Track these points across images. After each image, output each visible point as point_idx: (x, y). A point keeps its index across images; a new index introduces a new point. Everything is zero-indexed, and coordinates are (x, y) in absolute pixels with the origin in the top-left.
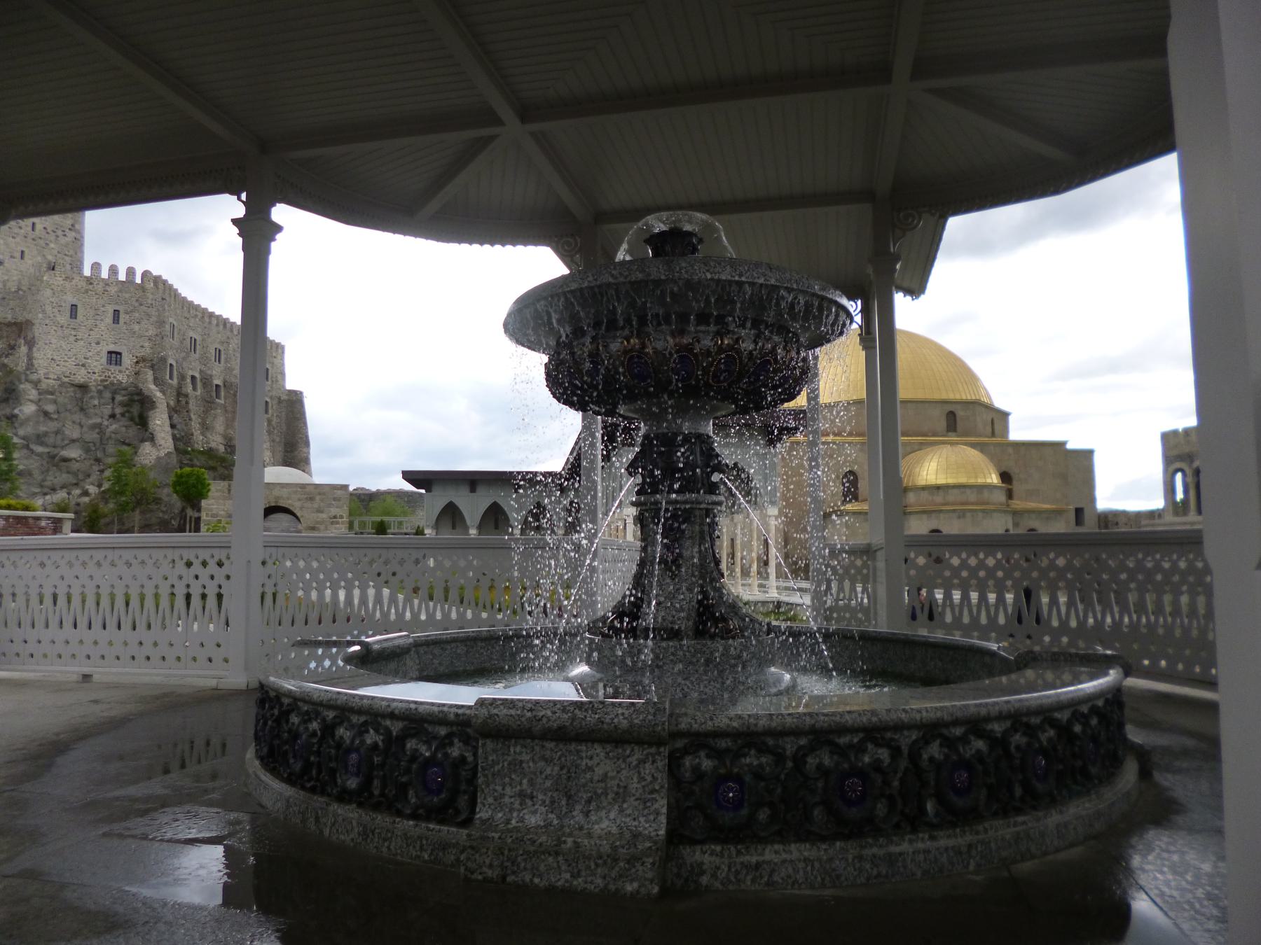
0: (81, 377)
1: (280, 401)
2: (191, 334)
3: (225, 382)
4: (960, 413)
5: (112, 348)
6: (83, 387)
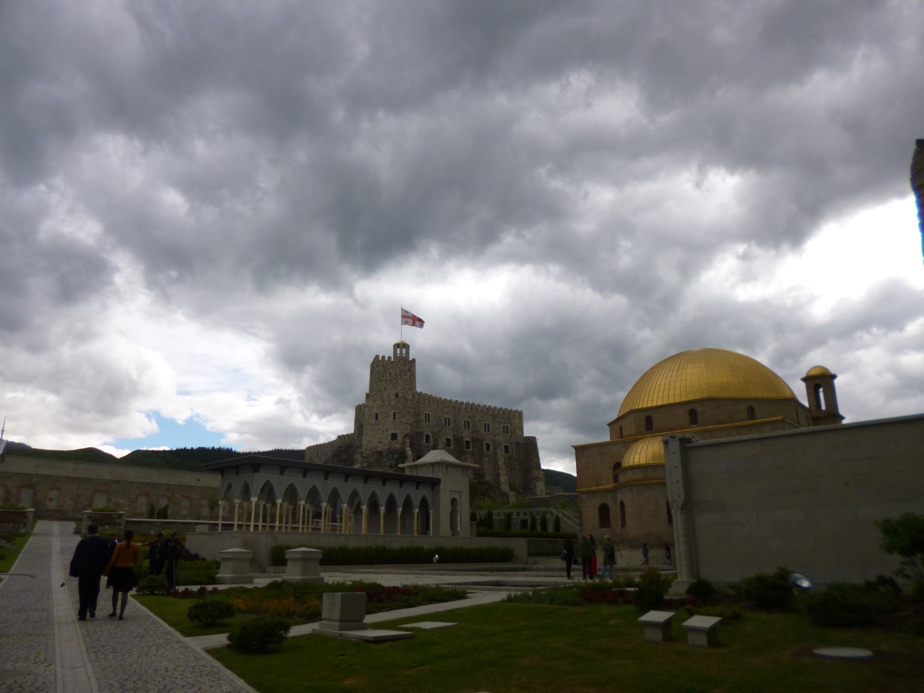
0: (380, 449)
1: (518, 444)
2: (446, 416)
3: (473, 439)
4: (699, 409)
5: (393, 431)
6: (380, 453)
